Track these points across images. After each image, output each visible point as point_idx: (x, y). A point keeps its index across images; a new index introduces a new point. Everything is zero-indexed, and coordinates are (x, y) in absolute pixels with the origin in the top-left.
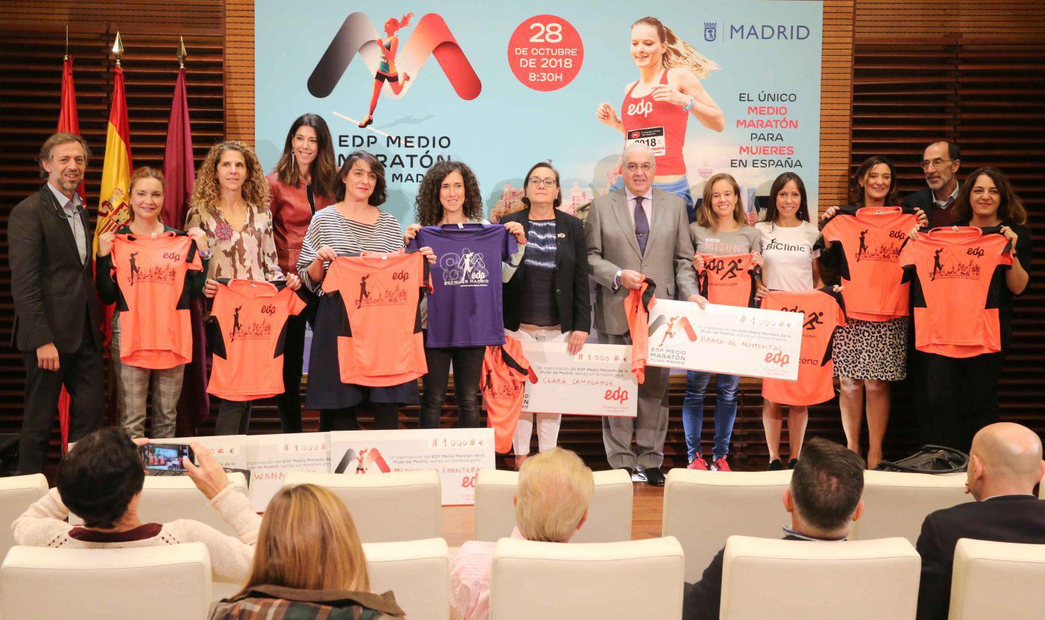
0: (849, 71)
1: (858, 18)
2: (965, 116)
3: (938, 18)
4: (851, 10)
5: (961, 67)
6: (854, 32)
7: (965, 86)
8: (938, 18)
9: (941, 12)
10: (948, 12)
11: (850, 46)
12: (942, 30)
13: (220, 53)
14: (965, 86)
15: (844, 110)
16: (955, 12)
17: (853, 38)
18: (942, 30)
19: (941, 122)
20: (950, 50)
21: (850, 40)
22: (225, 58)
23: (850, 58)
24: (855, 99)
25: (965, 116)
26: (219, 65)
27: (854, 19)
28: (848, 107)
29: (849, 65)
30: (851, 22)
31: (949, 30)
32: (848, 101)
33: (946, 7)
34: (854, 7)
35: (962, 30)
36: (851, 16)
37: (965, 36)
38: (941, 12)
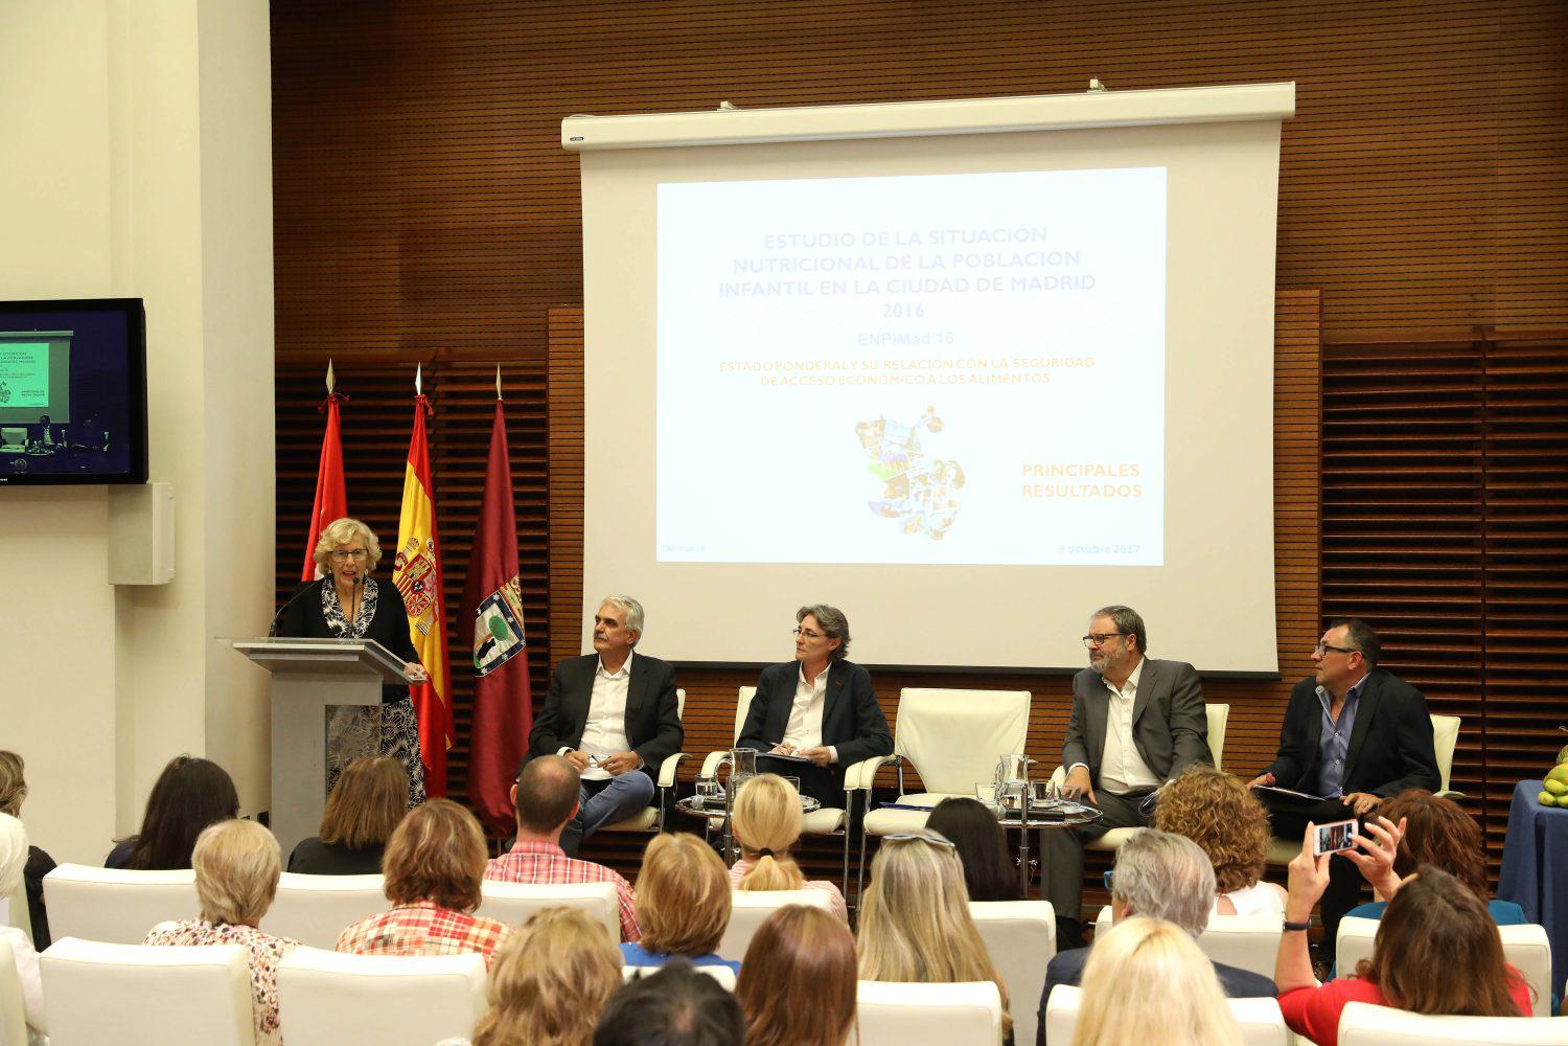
0: (1316, 381)
1: (1326, 310)
2: (1498, 437)
3: (1464, 306)
4: (1317, 301)
5: (1489, 372)
6: (1321, 329)
7: (1498, 396)
8: (1464, 306)
9: (1467, 298)
10: (1479, 297)
11: (1316, 349)
12: (1468, 321)
13: (543, 379)
14: (1498, 396)
15: (1309, 430)
16: (1484, 297)
17: (1321, 337)
18: (1468, 321)
19: (1469, 446)
20: (1481, 349)
21: (1316, 341)
24: (1327, 416)
25: (1498, 437)
26: (543, 394)
27: (1321, 313)
29: (1316, 372)
30: (1317, 317)
31: (1476, 321)
32: (1316, 420)
33: (1475, 290)
34: (1321, 297)
35: (1499, 320)
36: (1316, 309)
37: (1498, 328)
38: (1467, 298)
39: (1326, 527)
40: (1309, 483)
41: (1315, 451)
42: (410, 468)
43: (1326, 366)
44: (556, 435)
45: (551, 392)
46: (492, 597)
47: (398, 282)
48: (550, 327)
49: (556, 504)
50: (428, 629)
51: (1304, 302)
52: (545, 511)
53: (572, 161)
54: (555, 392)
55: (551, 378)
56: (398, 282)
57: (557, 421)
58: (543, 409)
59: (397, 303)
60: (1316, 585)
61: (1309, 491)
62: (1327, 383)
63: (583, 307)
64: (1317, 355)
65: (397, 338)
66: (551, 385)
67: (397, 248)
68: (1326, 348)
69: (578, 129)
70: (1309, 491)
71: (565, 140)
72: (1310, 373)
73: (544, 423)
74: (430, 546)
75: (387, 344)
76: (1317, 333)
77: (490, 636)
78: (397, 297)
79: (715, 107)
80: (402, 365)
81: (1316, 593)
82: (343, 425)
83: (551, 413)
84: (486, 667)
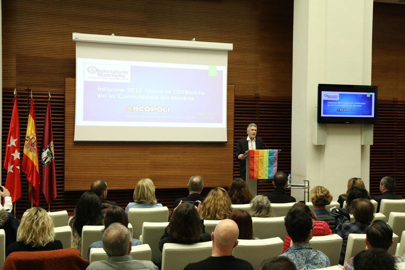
11: (234, 97)
15: (232, 113)
21: (233, 95)
22: (65, 97)
23: (233, 100)
24: (235, 110)
26: (64, 99)
28: (233, 112)
32: (233, 111)
39: (235, 132)
40: (232, 123)
41: (233, 117)
43: (235, 100)
44: (67, 109)
45: (66, 98)
49: (67, 126)
50: (35, 155)
52: (64, 127)
54: (67, 98)
55: (66, 95)
57: (67, 105)
58: (64, 102)
60: (233, 144)
61: (232, 125)
62: (235, 104)
64: (234, 98)
66: (66, 96)
68: (235, 97)
70: (232, 125)
72: (232, 102)
76: (234, 94)
81: (233, 145)
83: (66, 103)
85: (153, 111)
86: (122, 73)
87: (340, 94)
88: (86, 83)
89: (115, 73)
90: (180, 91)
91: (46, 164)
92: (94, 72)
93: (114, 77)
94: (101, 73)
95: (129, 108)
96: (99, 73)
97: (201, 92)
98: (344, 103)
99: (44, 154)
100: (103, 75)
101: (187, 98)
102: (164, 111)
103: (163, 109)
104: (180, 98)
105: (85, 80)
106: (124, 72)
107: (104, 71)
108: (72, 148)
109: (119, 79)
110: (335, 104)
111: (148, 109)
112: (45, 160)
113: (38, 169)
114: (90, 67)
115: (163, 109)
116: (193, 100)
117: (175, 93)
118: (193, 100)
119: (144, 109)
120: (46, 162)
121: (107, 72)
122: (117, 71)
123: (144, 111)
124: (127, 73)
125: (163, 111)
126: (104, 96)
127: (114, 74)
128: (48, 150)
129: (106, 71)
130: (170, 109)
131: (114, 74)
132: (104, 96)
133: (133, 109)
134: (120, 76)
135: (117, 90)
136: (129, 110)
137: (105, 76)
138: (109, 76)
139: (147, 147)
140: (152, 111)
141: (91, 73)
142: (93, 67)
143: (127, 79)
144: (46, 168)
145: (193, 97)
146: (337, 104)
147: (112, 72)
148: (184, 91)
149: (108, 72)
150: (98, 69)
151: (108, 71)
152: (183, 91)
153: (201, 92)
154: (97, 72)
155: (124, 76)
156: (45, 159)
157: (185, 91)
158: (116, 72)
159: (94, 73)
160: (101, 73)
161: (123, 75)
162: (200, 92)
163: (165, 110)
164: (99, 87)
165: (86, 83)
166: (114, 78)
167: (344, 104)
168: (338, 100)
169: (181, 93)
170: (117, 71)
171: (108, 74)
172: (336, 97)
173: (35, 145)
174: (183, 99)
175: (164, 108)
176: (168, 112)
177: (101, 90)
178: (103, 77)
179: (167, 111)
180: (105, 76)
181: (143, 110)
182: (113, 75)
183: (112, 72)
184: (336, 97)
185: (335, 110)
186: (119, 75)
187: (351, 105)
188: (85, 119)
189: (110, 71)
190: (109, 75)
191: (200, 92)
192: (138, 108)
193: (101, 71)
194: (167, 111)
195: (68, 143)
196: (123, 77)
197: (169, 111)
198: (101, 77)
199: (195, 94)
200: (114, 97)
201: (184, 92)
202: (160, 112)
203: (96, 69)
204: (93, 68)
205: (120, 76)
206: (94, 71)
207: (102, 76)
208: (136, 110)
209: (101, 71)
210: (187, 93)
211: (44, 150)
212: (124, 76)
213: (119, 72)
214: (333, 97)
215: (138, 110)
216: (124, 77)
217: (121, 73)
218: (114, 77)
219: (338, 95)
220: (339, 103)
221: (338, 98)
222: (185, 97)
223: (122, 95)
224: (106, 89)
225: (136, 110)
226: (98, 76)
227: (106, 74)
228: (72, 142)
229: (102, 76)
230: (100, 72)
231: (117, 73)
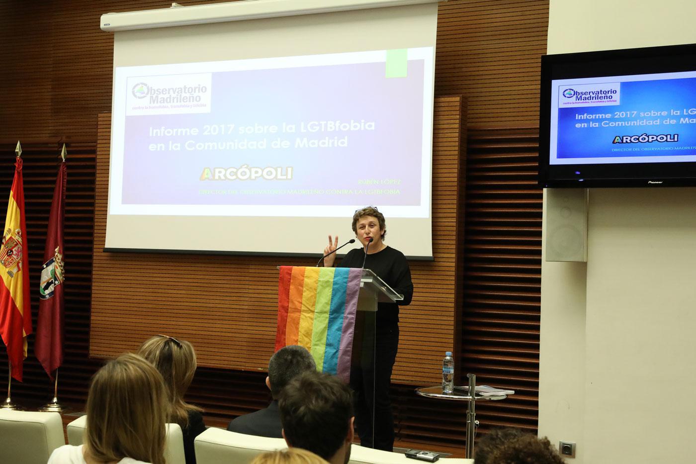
13: (94, 152)
26: (94, 160)
42: (12, 193)
46: (53, 259)
47: (50, 104)
48: (99, 123)
51: (451, 104)
53: (109, 37)
56: (50, 104)
58: (94, 167)
59: (50, 114)
63: (111, 113)
65: (49, 132)
67: (50, 87)
69: (109, 20)
71: (102, 26)
73: (94, 174)
74: (18, 233)
75: (44, 136)
77: (51, 278)
78: (50, 111)
79: (169, 6)
80: (50, 145)
82: (25, 175)
84: (48, 294)
85: (256, 177)
86: (195, 92)
87: (624, 85)
88: (130, 120)
89: (181, 93)
90: (317, 123)
91: (47, 296)
92: (144, 95)
93: (180, 102)
94: (155, 95)
95: (207, 171)
96: (152, 97)
97: (365, 124)
98: (642, 114)
99: (46, 274)
100: (159, 100)
101: (331, 141)
102: (279, 177)
103: (276, 171)
104: (316, 142)
105: (127, 115)
106: (199, 88)
107: (161, 91)
108: (105, 265)
109: (189, 106)
110: (606, 119)
111: (244, 173)
112: (46, 288)
113: (19, 304)
114: (137, 85)
115: (276, 171)
116: (346, 145)
117: (305, 131)
118: (346, 145)
119: (236, 174)
120: (47, 292)
121: (167, 92)
122: (185, 88)
123: (237, 178)
124: (203, 89)
125: (276, 177)
126: (161, 147)
127: (181, 95)
128: (51, 268)
129: (166, 90)
130: (292, 171)
131: (181, 95)
132: (161, 147)
133: (214, 176)
134: (191, 98)
135: (184, 130)
136: (206, 176)
137: (164, 102)
138: (170, 102)
139: (244, 267)
140: (254, 178)
141: (139, 98)
142: (142, 84)
143: (205, 105)
144: (47, 304)
145: (346, 138)
146: (612, 119)
147: (177, 90)
148: (326, 122)
149: (169, 93)
150: (151, 88)
151: (169, 90)
152: (323, 123)
153: (365, 124)
154: (149, 95)
155: (198, 98)
156: (45, 284)
157: (329, 122)
158: (183, 89)
159: (145, 96)
160: (155, 95)
161: (197, 97)
162: (363, 124)
163: (281, 175)
164: (151, 129)
165: (130, 120)
166: (179, 104)
167: (642, 119)
168: (618, 103)
169: (317, 128)
170: (185, 88)
171: (169, 96)
172: (610, 94)
173: (15, 253)
174: (324, 143)
175: (279, 170)
176: (287, 179)
177: (154, 135)
178: (159, 104)
179: (284, 177)
180: (164, 102)
181: (234, 177)
182: (177, 98)
183: (177, 90)
184: (606, 94)
185: (606, 140)
186: (190, 97)
187: (674, 117)
188: (126, 200)
189: (173, 89)
190: (170, 98)
191: (363, 124)
192: (223, 171)
193: (156, 92)
194: (284, 177)
195: (97, 254)
196: (196, 100)
197: (289, 177)
198: (156, 105)
199: (352, 129)
200: (179, 149)
201: (326, 125)
202: (266, 179)
203: (148, 88)
204: (141, 85)
205: (191, 98)
206: (144, 93)
207: (157, 103)
208: (219, 177)
209: (156, 92)
210: (331, 128)
211: (45, 266)
212: (198, 98)
213: (188, 91)
214: (598, 95)
215: (225, 175)
216: (199, 101)
217: (193, 93)
218: (180, 102)
219: (618, 88)
220: (618, 114)
221: (617, 97)
222: (327, 138)
223: (194, 142)
224: (164, 132)
225: (219, 177)
226: (150, 103)
227: (166, 96)
228: (102, 250)
229: (157, 103)
230: (154, 93)
231: (185, 92)
